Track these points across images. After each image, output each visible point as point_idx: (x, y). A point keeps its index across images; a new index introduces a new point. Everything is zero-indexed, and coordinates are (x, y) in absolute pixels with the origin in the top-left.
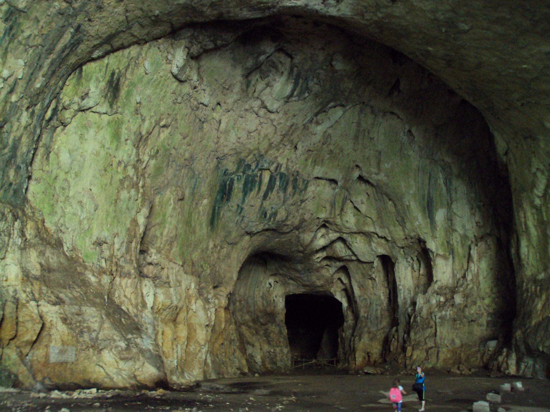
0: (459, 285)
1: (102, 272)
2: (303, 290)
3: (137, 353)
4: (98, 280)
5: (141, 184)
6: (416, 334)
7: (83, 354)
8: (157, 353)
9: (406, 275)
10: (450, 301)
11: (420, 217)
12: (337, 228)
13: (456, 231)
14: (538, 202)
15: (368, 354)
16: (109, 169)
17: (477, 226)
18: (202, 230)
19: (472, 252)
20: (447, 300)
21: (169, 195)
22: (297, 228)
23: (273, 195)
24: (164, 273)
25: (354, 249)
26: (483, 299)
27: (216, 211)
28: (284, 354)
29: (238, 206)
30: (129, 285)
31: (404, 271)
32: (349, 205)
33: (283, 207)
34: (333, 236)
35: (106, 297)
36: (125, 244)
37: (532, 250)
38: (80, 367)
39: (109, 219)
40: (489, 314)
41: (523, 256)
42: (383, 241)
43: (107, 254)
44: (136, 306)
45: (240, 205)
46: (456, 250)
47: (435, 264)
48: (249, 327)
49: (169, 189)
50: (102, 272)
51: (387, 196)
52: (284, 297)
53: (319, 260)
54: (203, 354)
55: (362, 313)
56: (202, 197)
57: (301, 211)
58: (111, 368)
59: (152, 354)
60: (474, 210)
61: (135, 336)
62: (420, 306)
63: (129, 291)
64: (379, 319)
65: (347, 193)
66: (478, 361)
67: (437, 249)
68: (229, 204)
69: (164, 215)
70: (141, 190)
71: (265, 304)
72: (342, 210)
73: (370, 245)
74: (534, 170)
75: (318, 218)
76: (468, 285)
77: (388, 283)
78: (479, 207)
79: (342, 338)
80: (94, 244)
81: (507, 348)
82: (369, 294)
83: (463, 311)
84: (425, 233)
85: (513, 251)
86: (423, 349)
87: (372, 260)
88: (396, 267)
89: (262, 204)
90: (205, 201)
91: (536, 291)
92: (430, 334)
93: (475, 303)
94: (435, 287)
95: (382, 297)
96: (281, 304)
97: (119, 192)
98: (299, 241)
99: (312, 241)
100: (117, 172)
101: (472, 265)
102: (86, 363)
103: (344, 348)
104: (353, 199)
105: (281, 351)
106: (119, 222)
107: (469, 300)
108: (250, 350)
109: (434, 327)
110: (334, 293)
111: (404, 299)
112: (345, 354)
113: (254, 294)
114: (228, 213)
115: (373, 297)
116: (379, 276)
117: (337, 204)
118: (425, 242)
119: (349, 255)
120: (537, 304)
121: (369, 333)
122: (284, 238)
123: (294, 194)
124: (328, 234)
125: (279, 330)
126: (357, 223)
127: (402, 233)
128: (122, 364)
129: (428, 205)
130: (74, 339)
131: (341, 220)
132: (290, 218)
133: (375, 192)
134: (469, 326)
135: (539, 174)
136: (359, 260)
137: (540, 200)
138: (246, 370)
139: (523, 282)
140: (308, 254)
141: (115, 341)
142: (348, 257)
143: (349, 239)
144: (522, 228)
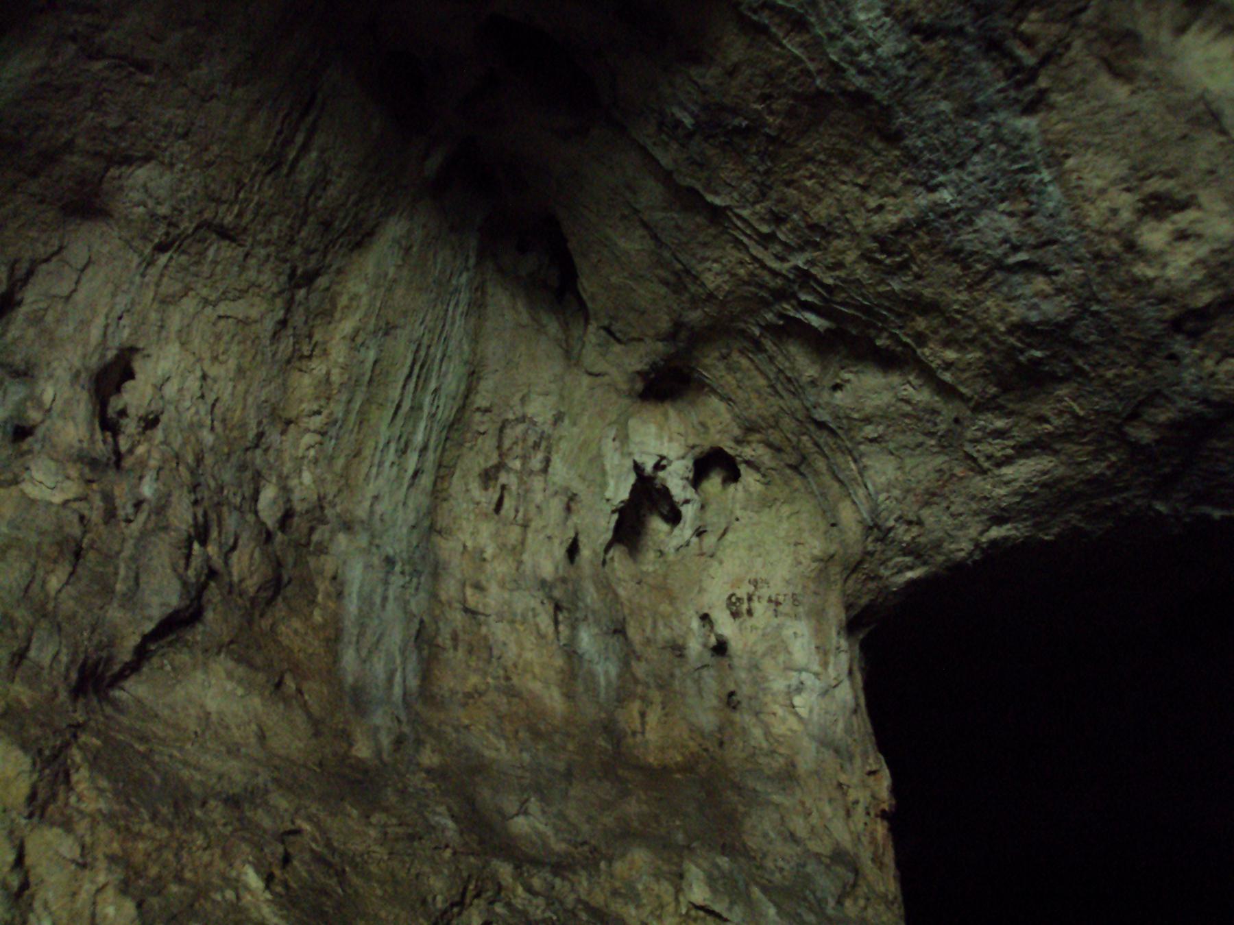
2: (1023, 471)
71: (606, 670)
96: (806, 686)
113: (430, 527)
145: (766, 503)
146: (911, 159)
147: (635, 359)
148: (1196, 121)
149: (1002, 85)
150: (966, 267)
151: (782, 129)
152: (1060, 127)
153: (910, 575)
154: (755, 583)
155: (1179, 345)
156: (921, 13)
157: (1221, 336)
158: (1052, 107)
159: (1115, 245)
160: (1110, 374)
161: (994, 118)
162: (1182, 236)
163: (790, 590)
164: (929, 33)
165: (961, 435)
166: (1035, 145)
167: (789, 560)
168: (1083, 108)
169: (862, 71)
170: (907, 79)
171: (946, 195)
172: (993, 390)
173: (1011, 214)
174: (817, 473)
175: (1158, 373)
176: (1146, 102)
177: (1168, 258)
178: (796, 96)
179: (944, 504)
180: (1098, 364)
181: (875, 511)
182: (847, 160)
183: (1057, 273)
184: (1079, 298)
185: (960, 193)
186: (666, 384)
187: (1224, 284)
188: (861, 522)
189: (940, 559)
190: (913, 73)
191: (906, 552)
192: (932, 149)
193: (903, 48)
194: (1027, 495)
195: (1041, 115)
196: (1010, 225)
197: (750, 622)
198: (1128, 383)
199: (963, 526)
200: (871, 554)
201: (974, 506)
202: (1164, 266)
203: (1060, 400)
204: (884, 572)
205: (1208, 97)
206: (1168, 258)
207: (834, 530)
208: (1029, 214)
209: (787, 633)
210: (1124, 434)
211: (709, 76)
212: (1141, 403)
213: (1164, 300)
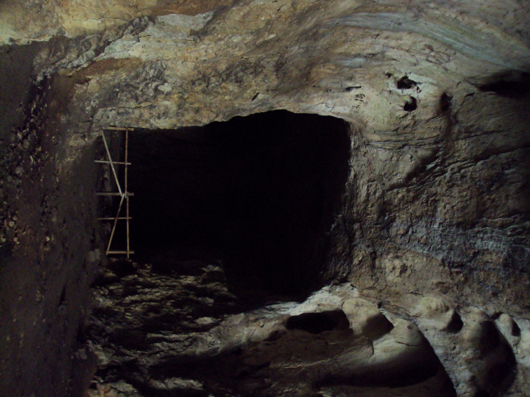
2: (363, 192)
145: (391, 115)
146: (450, 225)
147: (457, 98)
148: (418, 290)
149: (452, 260)
150: (417, 217)
151: (483, 198)
152: (434, 263)
153: (353, 143)
154: (367, 103)
155: (370, 250)
156: (481, 257)
157: (368, 259)
158: (440, 265)
159: (399, 254)
160: (373, 230)
161: (446, 251)
162: (394, 268)
163: (360, 112)
164: (476, 254)
165: (380, 182)
166: (434, 255)
167: (370, 115)
168: (436, 271)
169: (479, 232)
170: (468, 241)
171: (436, 226)
172: (386, 199)
173: (422, 237)
174: (392, 135)
175: (367, 241)
176: (429, 283)
177: (391, 262)
178: (487, 209)
179: (366, 165)
180: (376, 230)
181: (373, 146)
182: (463, 208)
183: (401, 237)
184: (393, 238)
185: (434, 230)
186: (445, 102)
187: (378, 268)
188: (371, 141)
189: (353, 154)
190: (469, 243)
191: (359, 146)
192: (449, 232)
193: (476, 246)
194: (357, 188)
195: (440, 262)
196: (419, 235)
197: (353, 99)
198: (369, 232)
199: (358, 166)
200: (362, 137)
201: (362, 173)
202: (389, 261)
203: (374, 214)
204: (356, 137)
205: (421, 296)
206: (391, 262)
207: (373, 131)
208: (419, 242)
209: (346, 108)
210: (358, 222)
211: (512, 189)
212: (363, 232)
213: (381, 255)
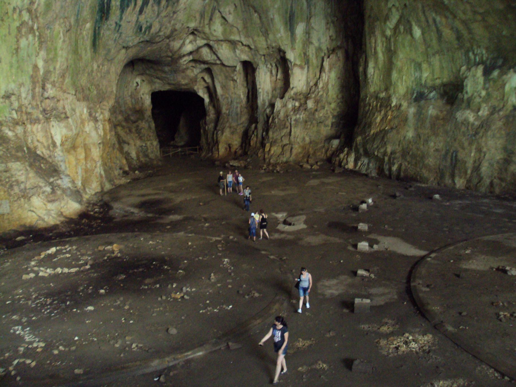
0: (311, 91)
1: (16, 123)
3: (61, 194)
4: (14, 134)
5: (35, 27)
6: (273, 133)
7: (16, 205)
8: (76, 189)
9: (266, 80)
10: (303, 105)
11: (282, 30)
12: (205, 36)
13: (312, 43)
14: (388, 33)
15: (230, 146)
16: (5, 18)
17: (330, 39)
18: (87, 54)
19: (324, 63)
20: (301, 105)
21: (58, 28)
22: (168, 37)
23: (148, 9)
24: (60, 104)
25: (219, 55)
26: (330, 104)
27: (97, 32)
28: (153, 146)
29: (116, 23)
30: (39, 130)
31: (263, 76)
32: (217, 15)
33: (157, 20)
34: (201, 42)
35: (25, 149)
36: (30, 92)
37: (377, 72)
38: (16, 216)
39: (14, 71)
40: (334, 117)
41: (369, 76)
42: (247, 49)
43: (16, 105)
44: (48, 148)
45: (118, 22)
46: (310, 61)
47: (292, 73)
48: (123, 127)
49: (58, 22)
50: (16, 123)
51: (254, 7)
52: (151, 93)
53: (185, 63)
54: (99, 170)
55: (224, 110)
56: (85, 21)
57: (172, 22)
58: (41, 211)
59: (71, 190)
60: (329, 25)
61: (56, 178)
62: (278, 109)
63: (40, 136)
64: (239, 116)
65: (215, 4)
66: (323, 155)
67: (295, 59)
68: (108, 23)
69: (56, 49)
70: (37, 34)
72: (211, 19)
73: (235, 52)
74: (390, 5)
75: (188, 27)
76: (319, 92)
77: (247, 84)
78: (333, 22)
79: (205, 130)
80: (3, 98)
81: (348, 148)
82: (230, 94)
83: (314, 114)
84: (286, 46)
85: (361, 69)
86: (279, 145)
87: (235, 65)
88: (257, 73)
89: (138, 18)
90: (88, 25)
91: (376, 106)
92: (285, 133)
93: (323, 108)
94: (291, 93)
95: (242, 96)
96: (148, 101)
97: (18, 41)
98: (169, 48)
99: (180, 48)
100: (14, 20)
101: (323, 75)
102: (20, 211)
103: (207, 139)
104: (222, 10)
105: (152, 144)
106: (22, 72)
107: (319, 105)
108: (126, 148)
109: (289, 128)
110: (197, 91)
111: (263, 100)
112: (208, 144)
113: (123, 94)
114: (107, 32)
115: (234, 96)
116: (239, 77)
117: (206, 15)
118: (284, 53)
119: (214, 60)
120: (377, 118)
121: (230, 127)
122: (155, 47)
123: (167, 7)
124: (195, 40)
125: (148, 125)
126: (224, 32)
127: (264, 43)
128: (50, 206)
129: (290, 20)
130: (6, 193)
131: (210, 29)
132: (162, 29)
133: (242, 4)
134: (317, 126)
135: (394, 10)
136: (223, 64)
137: (391, 32)
138: (127, 169)
139: (366, 97)
140: (174, 59)
141: (41, 187)
142: (212, 61)
143: (216, 46)
144: (372, 52)
